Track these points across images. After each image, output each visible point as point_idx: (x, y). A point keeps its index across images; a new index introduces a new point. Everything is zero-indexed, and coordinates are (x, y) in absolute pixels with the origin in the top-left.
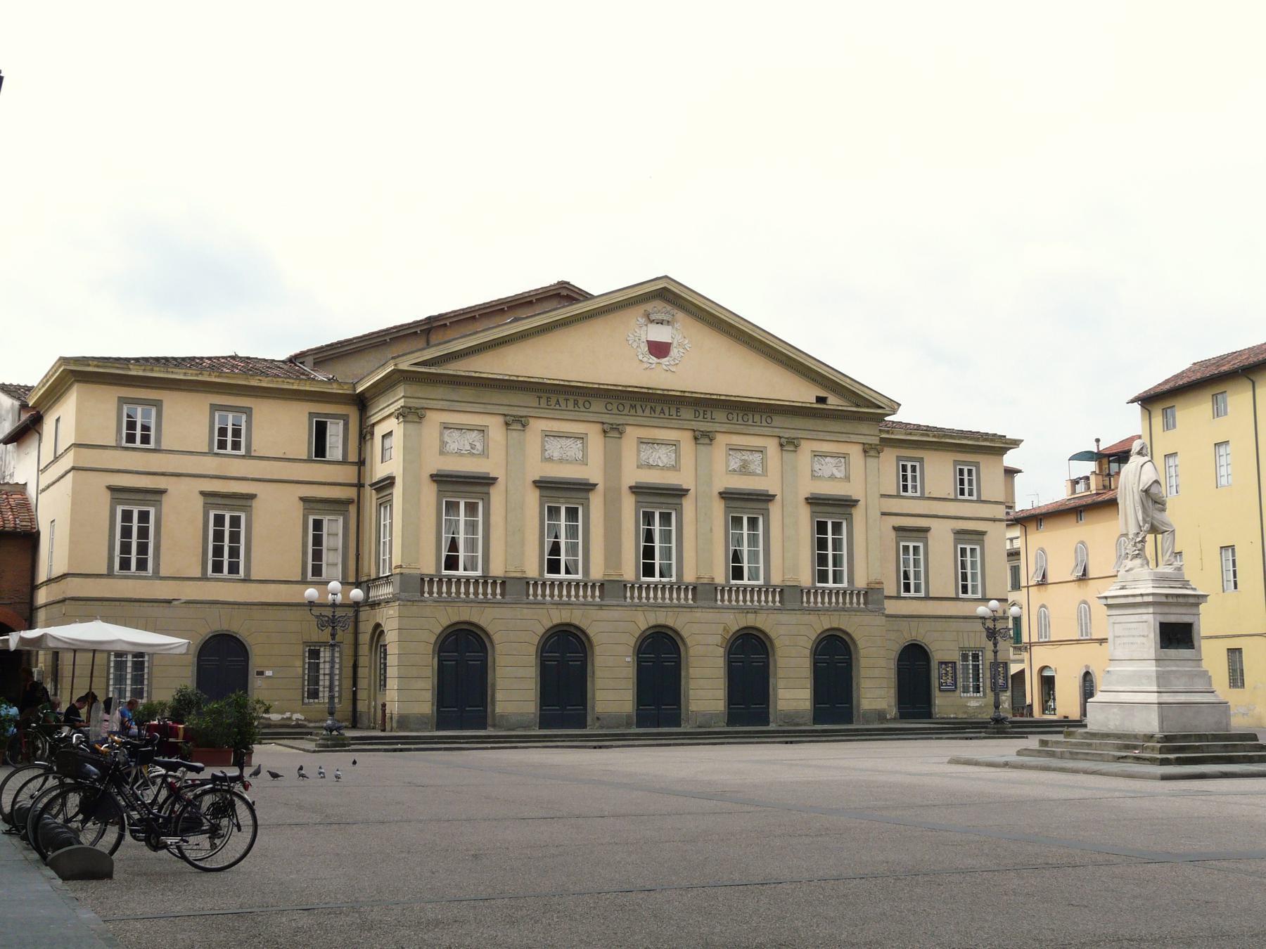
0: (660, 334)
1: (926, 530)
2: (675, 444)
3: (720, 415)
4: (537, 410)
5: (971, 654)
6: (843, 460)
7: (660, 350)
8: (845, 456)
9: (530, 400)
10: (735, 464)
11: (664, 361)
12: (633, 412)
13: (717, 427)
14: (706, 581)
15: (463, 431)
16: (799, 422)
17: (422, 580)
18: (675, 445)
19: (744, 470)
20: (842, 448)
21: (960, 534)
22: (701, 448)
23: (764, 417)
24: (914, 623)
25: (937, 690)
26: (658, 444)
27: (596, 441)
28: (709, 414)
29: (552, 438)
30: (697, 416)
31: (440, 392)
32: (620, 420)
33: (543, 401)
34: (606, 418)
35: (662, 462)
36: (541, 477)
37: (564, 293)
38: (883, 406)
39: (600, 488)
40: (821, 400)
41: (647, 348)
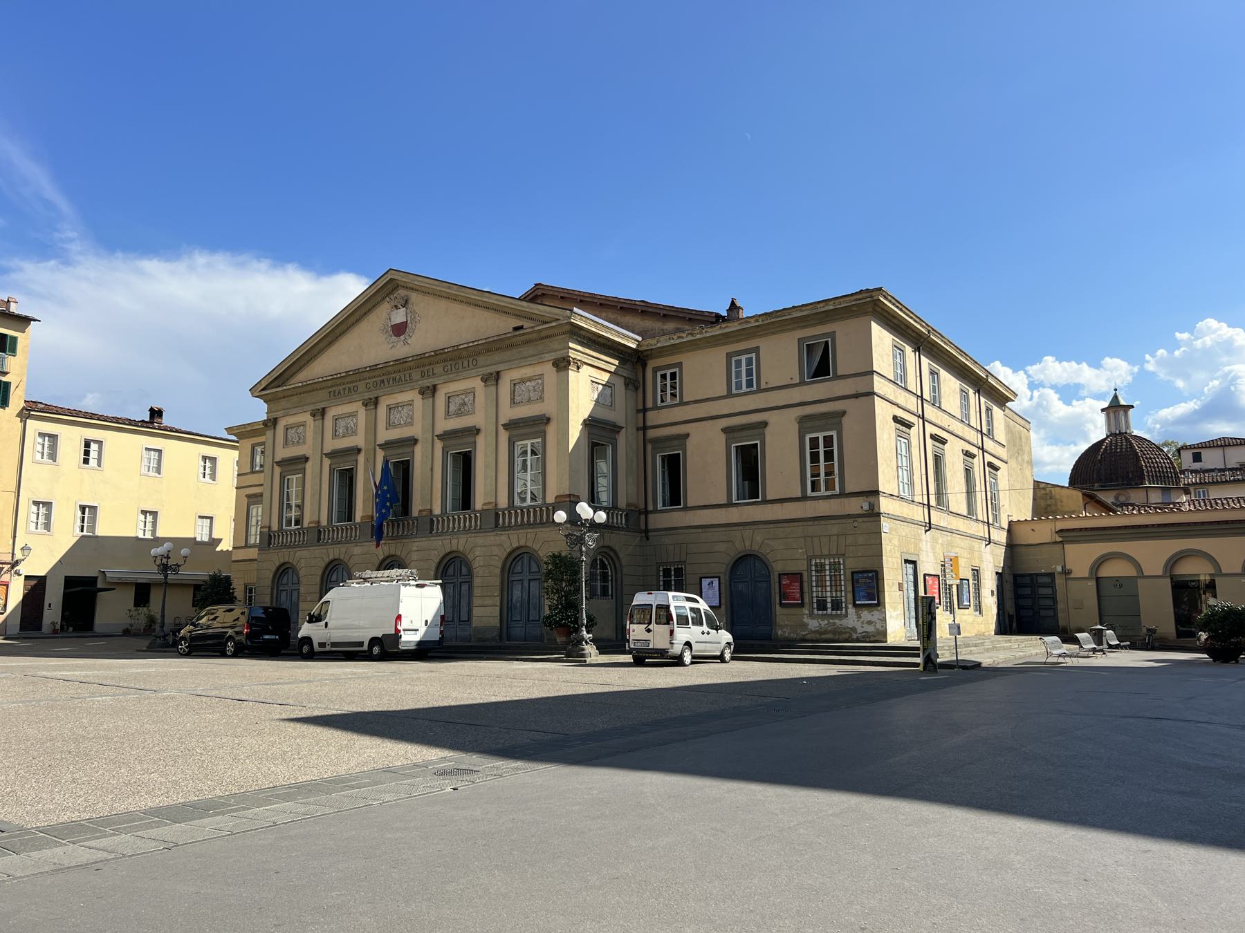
0: (399, 317)
1: (765, 424)
2: (411, 403)
3: (438, 369)
5: (673, 569)
6: (540, 381)
7: (399, 330)
8: (541, 376)
9: (323, 394)
10: (452, 408)
11: (402, 337)
12: (382, 385)
14: (424, 513)
16: (497, 357)
17: (270, 536)
18: (410, 405)
19: (459, 413)
20: (538, 370)
21: (806, 423)
22: (425, 401)
24: (747, 533)
25: (778, 606)
26: (401, 406)
27: (362, 414)
28: (431, 373)
29: (340, 420)
31: (284, 403)
33: (332, 394)
34: (367, 396)
35: (403, 420)
39: (363, 454)
40: (516, 329)
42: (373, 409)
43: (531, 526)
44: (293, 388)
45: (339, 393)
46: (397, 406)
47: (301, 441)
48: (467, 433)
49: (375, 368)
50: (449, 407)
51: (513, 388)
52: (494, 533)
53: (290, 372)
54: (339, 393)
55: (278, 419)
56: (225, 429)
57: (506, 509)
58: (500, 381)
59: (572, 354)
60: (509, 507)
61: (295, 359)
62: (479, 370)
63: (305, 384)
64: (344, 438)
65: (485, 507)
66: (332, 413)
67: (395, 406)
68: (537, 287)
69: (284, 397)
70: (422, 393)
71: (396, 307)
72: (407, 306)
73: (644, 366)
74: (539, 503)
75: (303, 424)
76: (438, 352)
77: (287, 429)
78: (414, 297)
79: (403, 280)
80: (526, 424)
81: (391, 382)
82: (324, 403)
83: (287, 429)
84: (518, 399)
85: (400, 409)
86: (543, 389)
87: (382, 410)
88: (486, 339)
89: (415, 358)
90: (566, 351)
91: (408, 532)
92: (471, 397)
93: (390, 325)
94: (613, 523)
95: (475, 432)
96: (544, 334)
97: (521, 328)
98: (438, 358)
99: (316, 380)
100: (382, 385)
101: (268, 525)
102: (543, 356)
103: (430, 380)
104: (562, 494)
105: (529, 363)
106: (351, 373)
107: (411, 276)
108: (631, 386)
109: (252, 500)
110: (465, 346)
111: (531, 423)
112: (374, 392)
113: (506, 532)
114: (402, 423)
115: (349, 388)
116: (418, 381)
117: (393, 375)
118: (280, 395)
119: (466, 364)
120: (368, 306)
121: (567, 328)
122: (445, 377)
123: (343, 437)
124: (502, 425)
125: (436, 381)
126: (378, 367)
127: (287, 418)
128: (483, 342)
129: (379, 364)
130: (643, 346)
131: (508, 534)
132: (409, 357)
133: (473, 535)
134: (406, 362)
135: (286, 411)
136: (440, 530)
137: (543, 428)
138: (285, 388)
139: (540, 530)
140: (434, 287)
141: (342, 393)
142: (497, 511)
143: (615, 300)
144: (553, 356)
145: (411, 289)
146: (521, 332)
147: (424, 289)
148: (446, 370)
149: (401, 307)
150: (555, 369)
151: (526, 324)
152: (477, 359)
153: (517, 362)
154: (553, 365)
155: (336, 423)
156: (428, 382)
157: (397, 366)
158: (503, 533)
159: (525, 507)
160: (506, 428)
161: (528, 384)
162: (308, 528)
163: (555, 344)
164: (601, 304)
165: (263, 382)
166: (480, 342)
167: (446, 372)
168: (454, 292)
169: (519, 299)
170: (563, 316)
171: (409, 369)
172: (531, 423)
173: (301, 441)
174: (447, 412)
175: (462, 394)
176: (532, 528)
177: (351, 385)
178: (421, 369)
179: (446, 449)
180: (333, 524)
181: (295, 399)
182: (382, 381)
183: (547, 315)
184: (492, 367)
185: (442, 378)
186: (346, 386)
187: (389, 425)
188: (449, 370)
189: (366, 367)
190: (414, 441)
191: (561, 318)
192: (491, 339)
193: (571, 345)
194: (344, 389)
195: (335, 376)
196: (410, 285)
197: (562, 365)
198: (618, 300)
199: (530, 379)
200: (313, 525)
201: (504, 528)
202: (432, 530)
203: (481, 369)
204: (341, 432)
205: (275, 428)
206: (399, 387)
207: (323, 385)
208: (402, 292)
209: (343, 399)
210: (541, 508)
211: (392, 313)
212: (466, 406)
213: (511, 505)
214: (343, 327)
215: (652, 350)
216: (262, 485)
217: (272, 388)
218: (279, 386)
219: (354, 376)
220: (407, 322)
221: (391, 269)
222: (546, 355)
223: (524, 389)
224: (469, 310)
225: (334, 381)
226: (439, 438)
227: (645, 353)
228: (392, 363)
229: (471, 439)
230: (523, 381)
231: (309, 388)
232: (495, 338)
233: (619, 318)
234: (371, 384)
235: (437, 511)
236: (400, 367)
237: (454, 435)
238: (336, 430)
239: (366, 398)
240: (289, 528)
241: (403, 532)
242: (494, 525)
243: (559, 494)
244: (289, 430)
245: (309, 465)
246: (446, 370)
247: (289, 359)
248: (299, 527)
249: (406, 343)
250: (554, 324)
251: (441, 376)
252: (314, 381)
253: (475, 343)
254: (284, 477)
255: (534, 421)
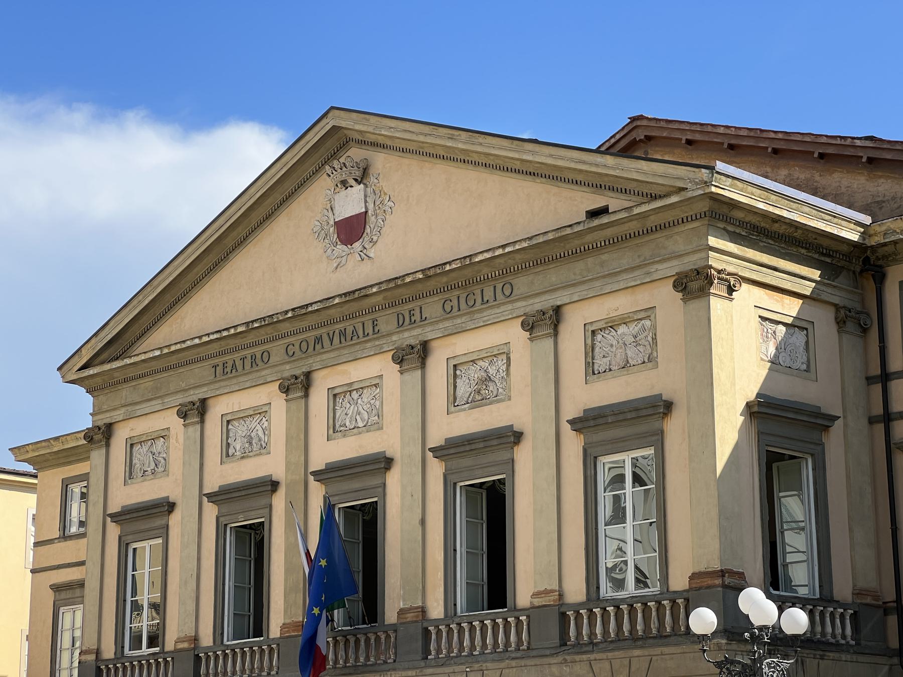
2: (376, 383)
3: (432, 307)
4: (212, 387)
6: (647, 323)
9: (202, 371)
10: (464, 389)
11: (357, 245)
12: (318, 347)
13: (428, 333)
14: (410, 617)
15: (149, 443)
16: (555, 275)
18: (376, 385)
22: (407, 376)
23: (499, 287)
28: (417, 317)
30: (401, 323)
31: (126, 393)
32: (299, 369)
34: (288, 370)
36: (220, 487)
37: (640, 135)
38: (680, 184)
40: (593, 214)
41: (336, 236)
42: (301, 397)
43: (640, 643)
44: (143, 361)
45: (234, 365)
46: (350, 389)
47: (159, 468)
48: (495, 442)
49: (303, 311)
50: (455, 387)
51: (589, 342)
52: (559, 659)
53: (136, 329)
54: (234, 365)
55: (116, 427)
56: (9, 449)
57: (581, 605)
58: (562, 328)
59: (716, 261)
60: (588, 599)
61: (146, 302)
62: (519, 304)
63: (166, 351)
64: (245, 461)
65: (537, 602)
66: (219, 408)
67: (345, 389)
68: (635, 124)
69: (126, 381)
70: (399, 359)
71: (344, 184)
72: (365, 181)
73: (880, 278)
74: (654, 589)
75: (164, 435)
76: (431, 272)
77: (132, 445)
78: (380, 161)
79: (357, 127)
80: (621, 417)
81: (336, 340)
82: (205, 389)
83: (132, 445)
84: (601, 363)
85: (355, 395)
86: (654, 339)
87: (319, 399)
88: (530, 239)
89: (384, 287)
90: (703, 255)
91: (377, 657)
92: (501, 363)
93: (332, 222)
94: (823, 633)
95: (512, 439)
96: (653, 221)
97: (604, 211)
98: (432, 284)
99: (189, 343)
100: (318, 347)
101: (96, 647)
102: (653, 268)
103: (415, 332)
104: (703, 570)
105: (622, 285)
106: (256, 325)
107: (373, 119)
108: (850, 326)
109: (64, 595)
110: (487, 255)
111: (633, 415)
112: (302, 363)
113: (585, 657)
114: (361, 424)
115: (254, 358)
116: (390, 334)
117: (341, 326)
118: (118, 376)
119: (489, 293)
120: (289, 185)
121: (704, 206)
122: (447, 324)
123: (243, 458)
124: (567, 421)
125: (428, 333)
126: (310, 309)
127: (132, 423)
128: (525, 245)
129: (311, 304)
130: (875, 234)
131: (590, 661)
132: (372, 286)
133: (514, 663)
134: (366, 296)
135: (130, 408)
136: (444, 651)
137: (656, 425)
138: (128, 361)
139: (658, 651)
140: (421, 138)
141: (240, 368)
142: (562, 610)
143: (808, 139)
144: (673, 268)
145: (375, 145)
146: (605, 219)
147: (397, 144)
148: (448, 309)
149: (353, 183)
150: (680, 295)
151: (614, 202)
152: (513, 282)
153: (597, 284)
154: (674, 286)
155: (228, 431)
156: (411, 337)
157: (347, 306)
158: (577, 658)
159: (623, 600)
160: (579, 426)
161: (622, 329)
162: (176, 651)
163: (677, 242)
164: (775, 151)
165: (84, 351)
166: (517, 247)
167: (448, 314)
168: (461, 146)
169: (597, 151)
170: (692, 181)
171: (372, 310)
172: (633, 415)
173: (159, 468)
174: (451, 398)
175: (482, 359)
176: (642, 647)
177: (257, 351)
178: (398, 309)
179: (452, 478)
180: (226, 642)
181: (147, 384)
182: (319, 340)
183: (660, 181)
184: (547, 297)
185: (441, 326)
186: (247, 352)
187: (334, 430)
188: (455, 309)
189: (286, 312)
190: (385, 462)
191: (689, 186)
192: (541, 239)
193: (713, 241)
194: (243, 359)
195: (225, 334)
196: (372, 138)
197: (694, 285)
198: (815, 139)
199: (625, 321)
200: (185, 645)
201: (580, 647)
202: (426, 652)
203: (524, 303)
204: (238, 448)
205: (108, 445)
206: (353, 349)
207: (203, 352)
208: (355, 153)
209: (241, 379)
210: (659, 603)
211: (337, 197)
212: (490, 384)
213: (594, 595)
214: (241, 231)
215: (895, 242)
216: (82, 563)
217: (102, 363)
218: (117, 359)
219: (262, 331)
220: (366, 212)
221: (332, 108)
222: (659, 266)
223: (615, 342)
224: (493, 181)
225: (223, 343)
226: (438, 454)
227: (881, 252)
228: (337, 301)
229: (503, 455)
230: (612, 325)
231: (174, 360)
232: (550, 236)
233: (817, 178)
234: (297, 346)
235: (436, 611)
236: (353, 307)
237: (468, 448)
238: (228, 445)
239: (287, 374)
240: (136, 653)
241: (367, 658)
242: (557, 641)
243: (697, 570)
244: (136, 448)
245: (175, 520)
246: (448, 309)
247: (135, 302)
248: (157, 649)
249: (364, 256)
250: (674, 199)
251: (437, 322)
252: (184, 346)
253: (508, 250)
254: (127, 544)
255: (637, 410)
